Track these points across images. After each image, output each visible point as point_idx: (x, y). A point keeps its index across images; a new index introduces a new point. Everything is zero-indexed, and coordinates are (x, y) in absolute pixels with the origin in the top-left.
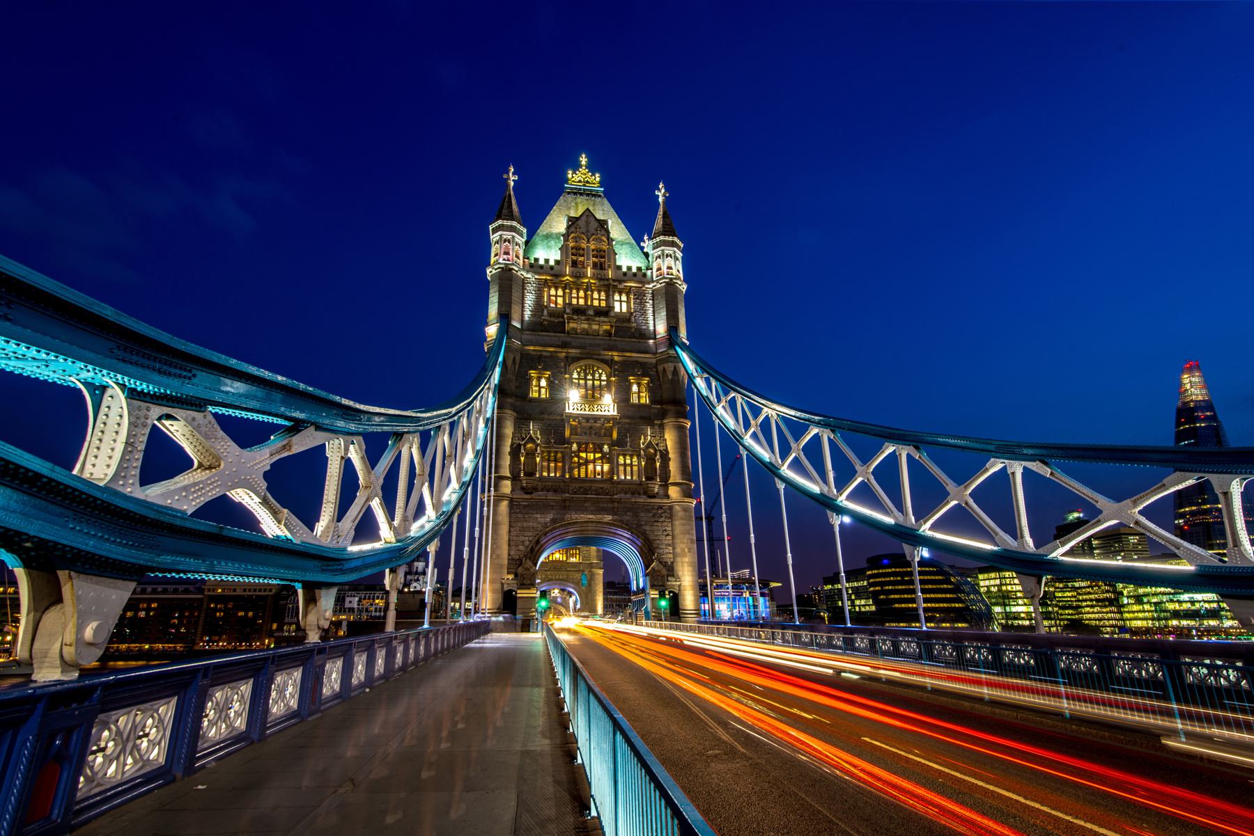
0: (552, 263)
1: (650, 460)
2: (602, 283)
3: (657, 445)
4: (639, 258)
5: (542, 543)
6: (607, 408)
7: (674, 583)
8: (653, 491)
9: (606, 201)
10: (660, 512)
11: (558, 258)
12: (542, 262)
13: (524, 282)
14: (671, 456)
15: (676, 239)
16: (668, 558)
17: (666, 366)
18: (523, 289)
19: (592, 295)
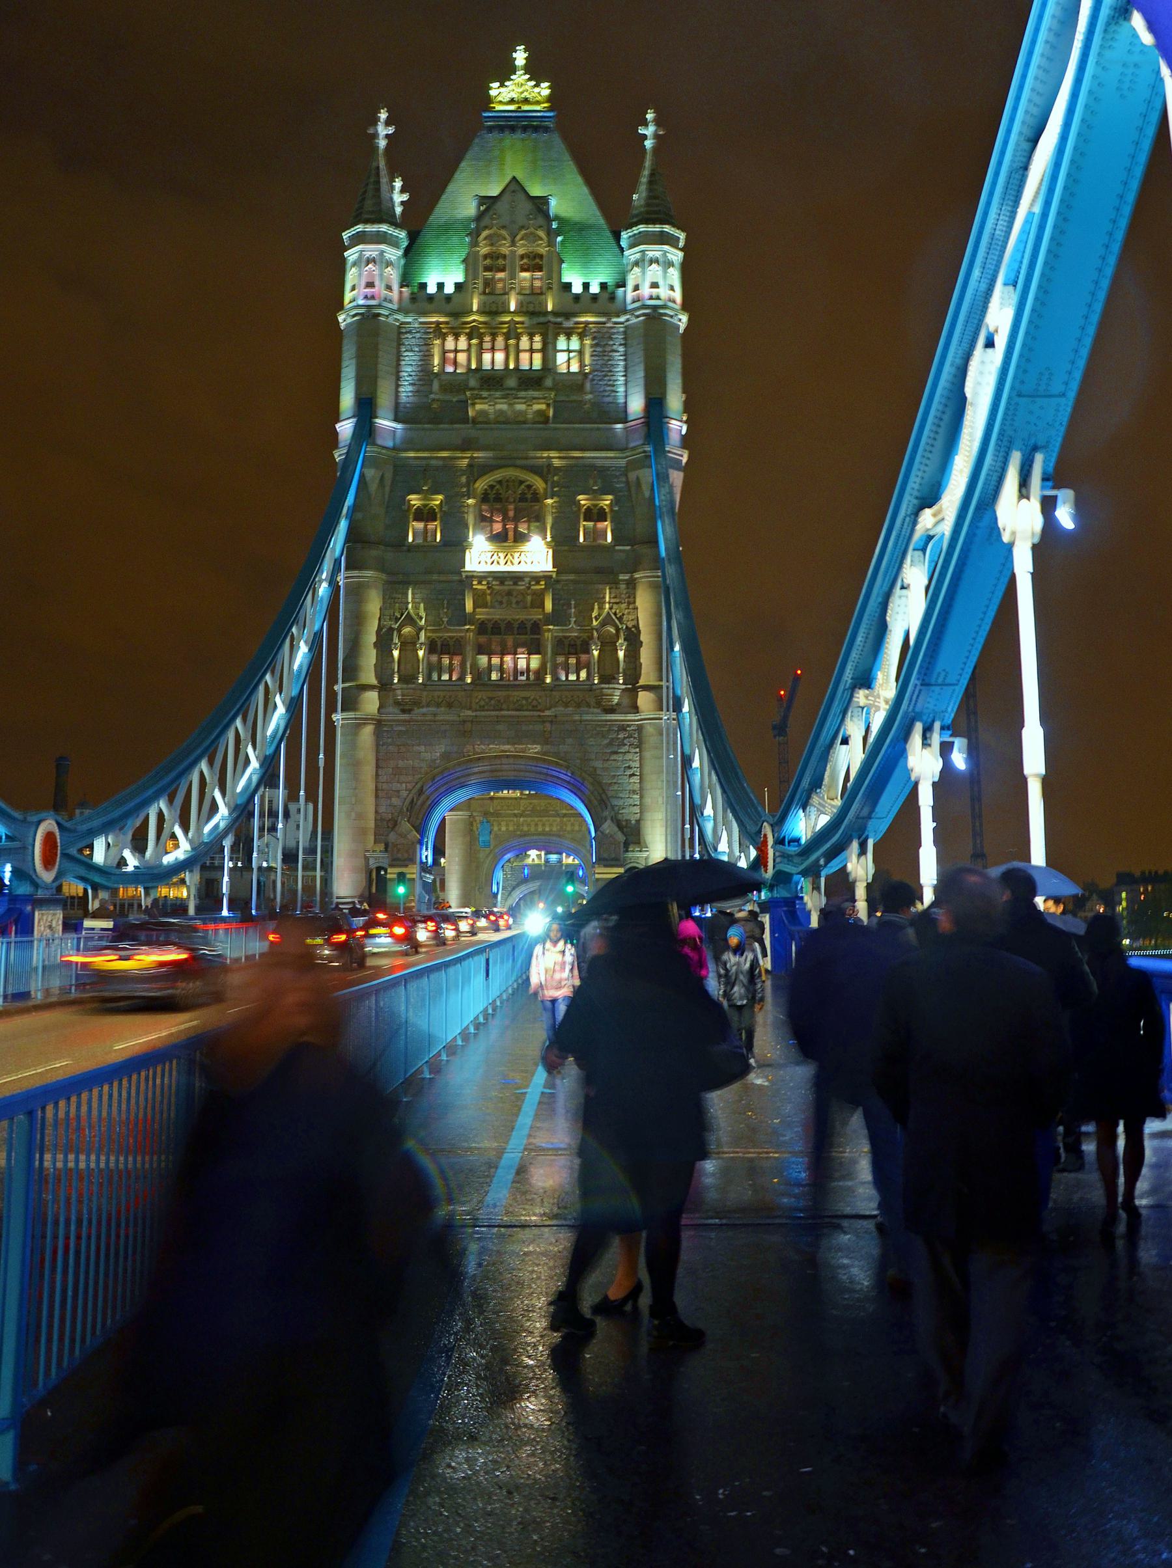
0: (449, 289)
2: (536, 320)
3: (620, 619)
9: (556, 139)
10: (621, 736)
11: (461, 279)
12: (432, 289)
13: (400, 331)
14: (642, 638)
15: (667, 228)
16: (631, 814)
18: (400, 344)
19: (517, 345)
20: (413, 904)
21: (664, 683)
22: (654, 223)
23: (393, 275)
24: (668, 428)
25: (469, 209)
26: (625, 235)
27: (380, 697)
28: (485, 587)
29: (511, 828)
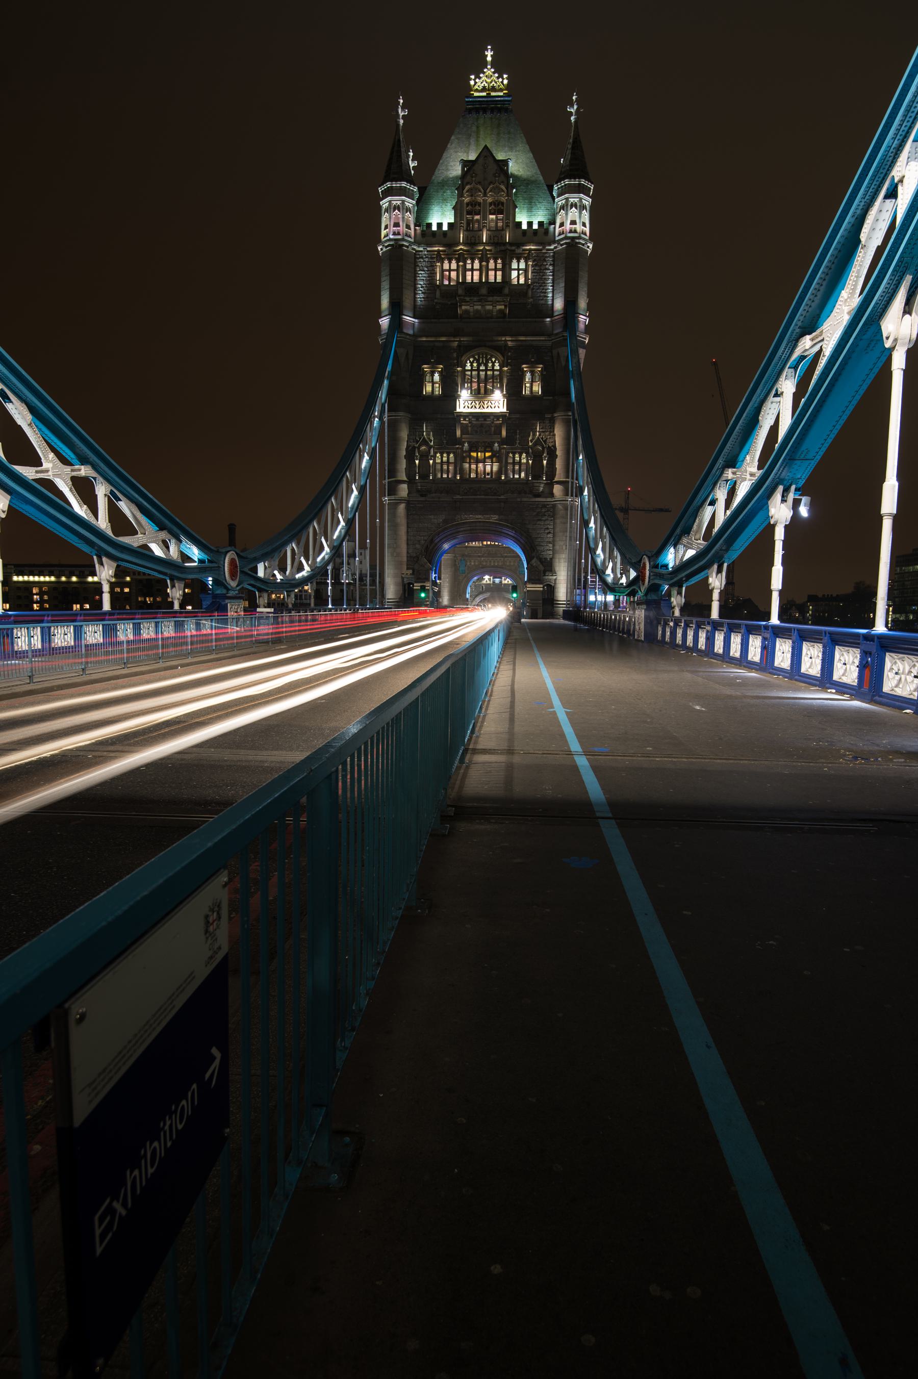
0: (445, 228)
1: (537, 458)
2: (499, 249)
4: (545, 203)
5: (436, 541)
6: (497, 404)
7: (551, 577)
8: (538, 490)
10: (543, 510)
11: (452, 221)
12: (434, 228)
13: (416, 256)
14: (559, 453)
15: (583, 182)
18: (416, 265)
19: (487, 265)
21: (570, 480)
23: (411, 218)
24: (578, 320)
25: (456, 170)
27: (408, 488)
28: (467, 422)
29: (477, 564)
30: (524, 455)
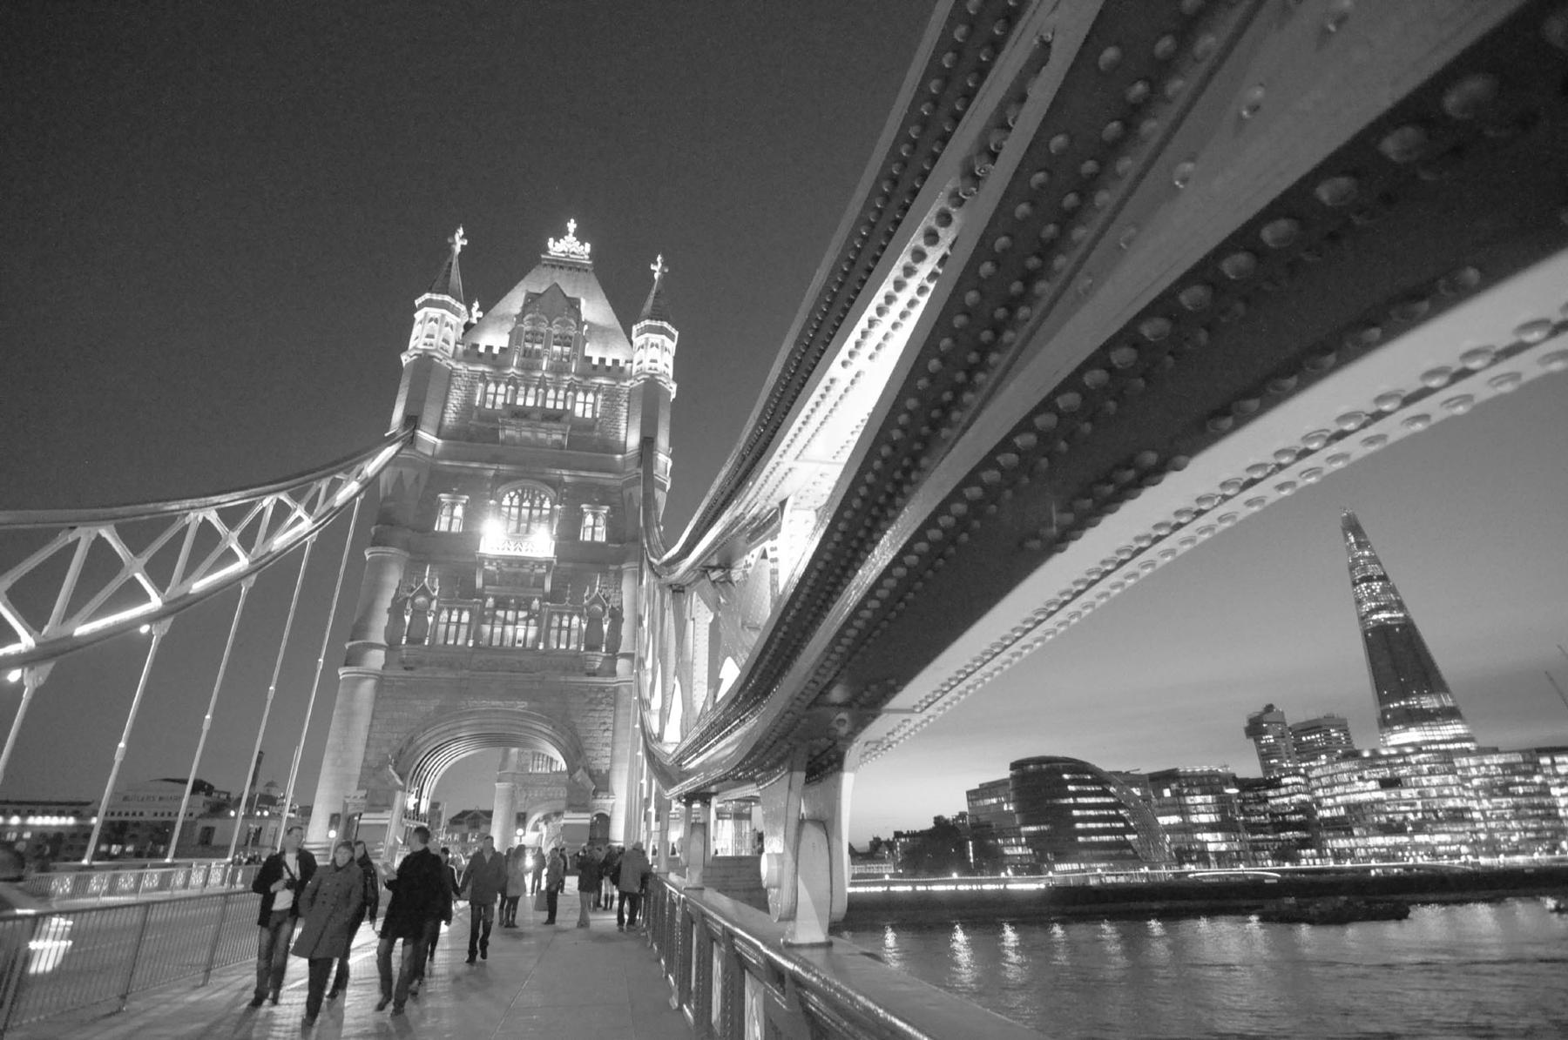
0: (496, 351)
1: (595, 622)
3: (607, 600)
5: (419, 742)
9: (593, 276)
10: (599, 696)
11: (506, 345)
12: (482, 349)
13: (451, 375)
14: (625, 615)
15: (665, 324)
16: (603, 764)
17: (632, 489)
18: (450, 382)
20: (381, 850)
22: (657, 320)
23: (454, 335)
26: (635, 328)
27: (386, 656)
29: (541, 795)
30: (576, 620)
